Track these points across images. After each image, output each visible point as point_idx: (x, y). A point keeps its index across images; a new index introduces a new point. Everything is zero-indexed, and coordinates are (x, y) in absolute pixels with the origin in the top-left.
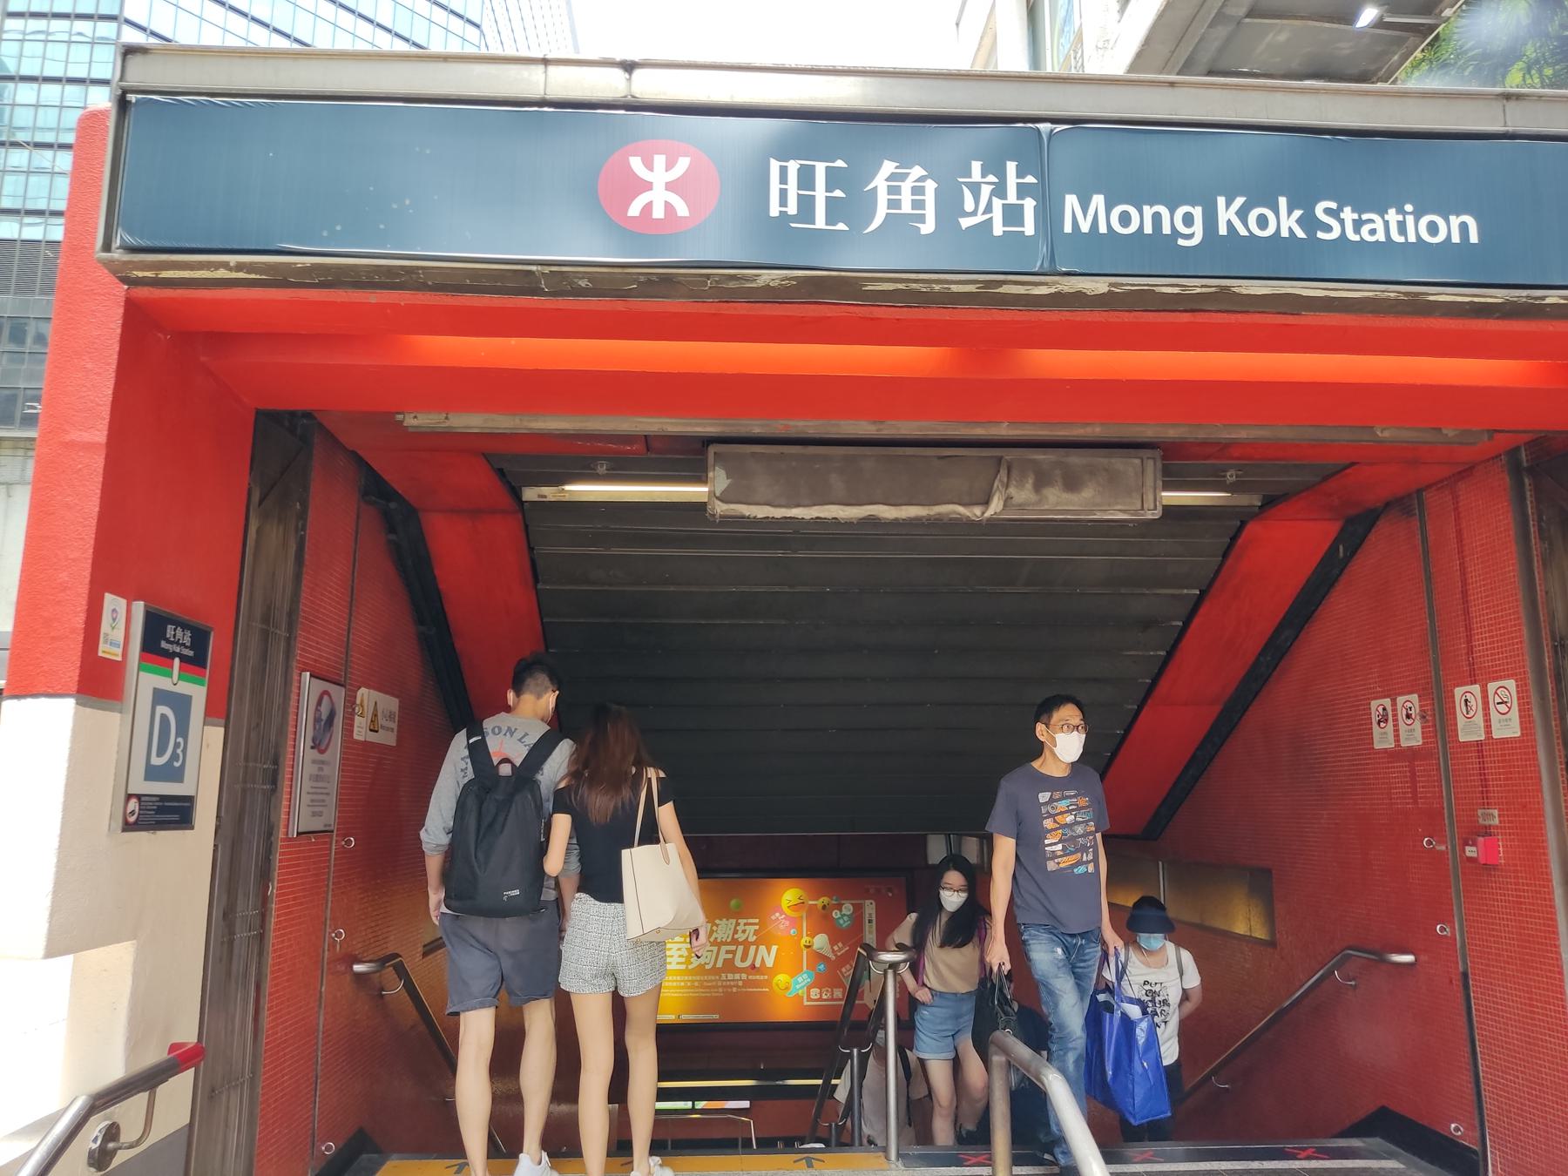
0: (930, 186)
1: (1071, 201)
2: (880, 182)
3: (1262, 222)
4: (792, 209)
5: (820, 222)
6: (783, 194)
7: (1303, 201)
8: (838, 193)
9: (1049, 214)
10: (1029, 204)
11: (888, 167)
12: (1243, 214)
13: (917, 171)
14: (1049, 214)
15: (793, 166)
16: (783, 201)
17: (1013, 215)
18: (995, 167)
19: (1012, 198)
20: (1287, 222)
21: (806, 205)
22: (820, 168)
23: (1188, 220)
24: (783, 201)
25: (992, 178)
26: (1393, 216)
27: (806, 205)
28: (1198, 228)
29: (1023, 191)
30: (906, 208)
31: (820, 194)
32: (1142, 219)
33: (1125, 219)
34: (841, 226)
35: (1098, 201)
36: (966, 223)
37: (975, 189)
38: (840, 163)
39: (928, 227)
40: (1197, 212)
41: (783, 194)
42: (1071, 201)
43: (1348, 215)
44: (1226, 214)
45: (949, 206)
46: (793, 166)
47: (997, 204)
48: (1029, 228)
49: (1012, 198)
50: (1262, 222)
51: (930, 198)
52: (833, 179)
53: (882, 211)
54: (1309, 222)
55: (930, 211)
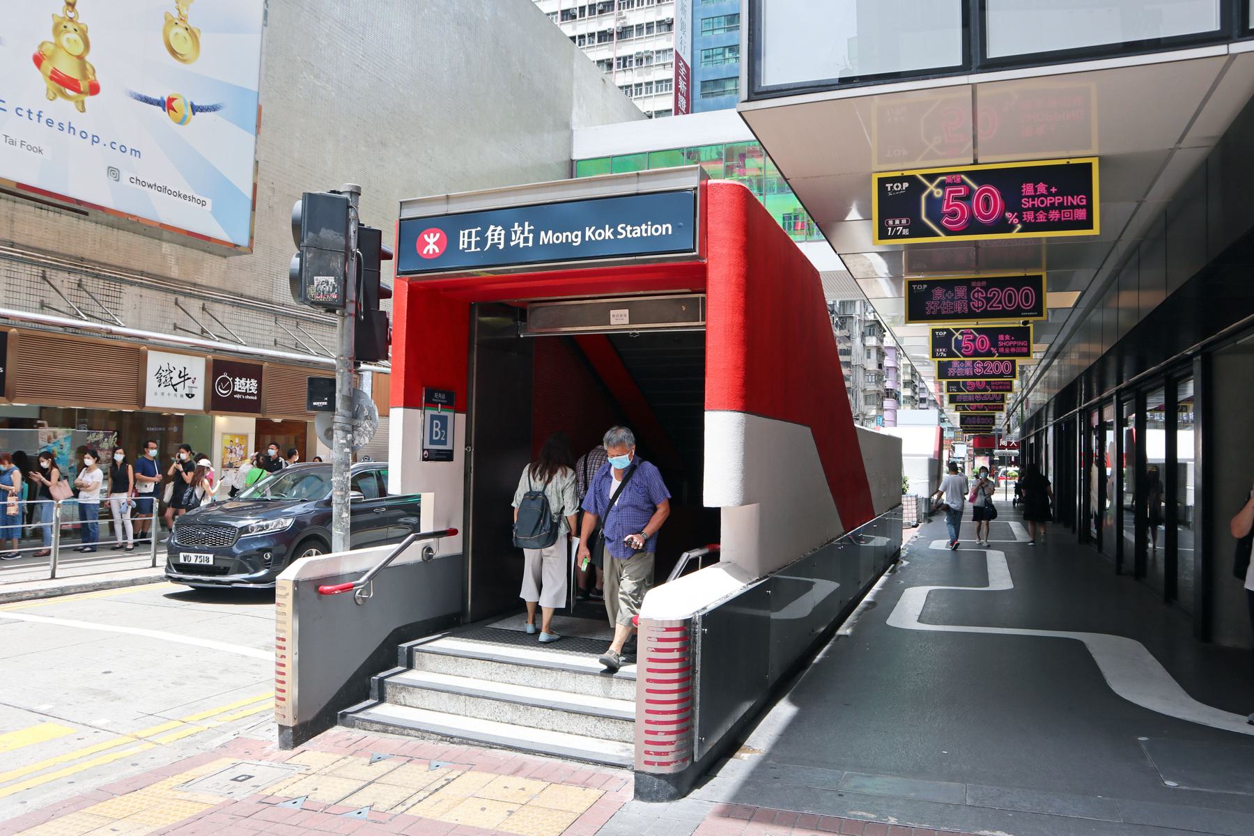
1: (543, 233)
2: (489, 233)
3: (600, 235)
7: (614, 226)
9: (537, 238)
10: (531, 236)
11: (492, 227)
12: (594, 233)
14: (537, 238)
20: (608, 234)
21: (469, 243)
22: (474, 231)
23: (576, 236)
26: (644, 227)
27: (469, 243)
28: (579, 239)
29: (529, 232)
31: (473, 240)
32: (562, 237)
33: (558, 238)
35: (550, 232)
36: (512, 244)
39: (501, 247)
40: (579, 233)
42: (543, 233)
43: (629, 228)
44: (588, 233)
45: (508, 239)
48: (530, 244)
50: (600, 235)
51: (502, 237)
52: (477, 234)
53: (490, 242)
54: (616, 233)
55: (502, 241)
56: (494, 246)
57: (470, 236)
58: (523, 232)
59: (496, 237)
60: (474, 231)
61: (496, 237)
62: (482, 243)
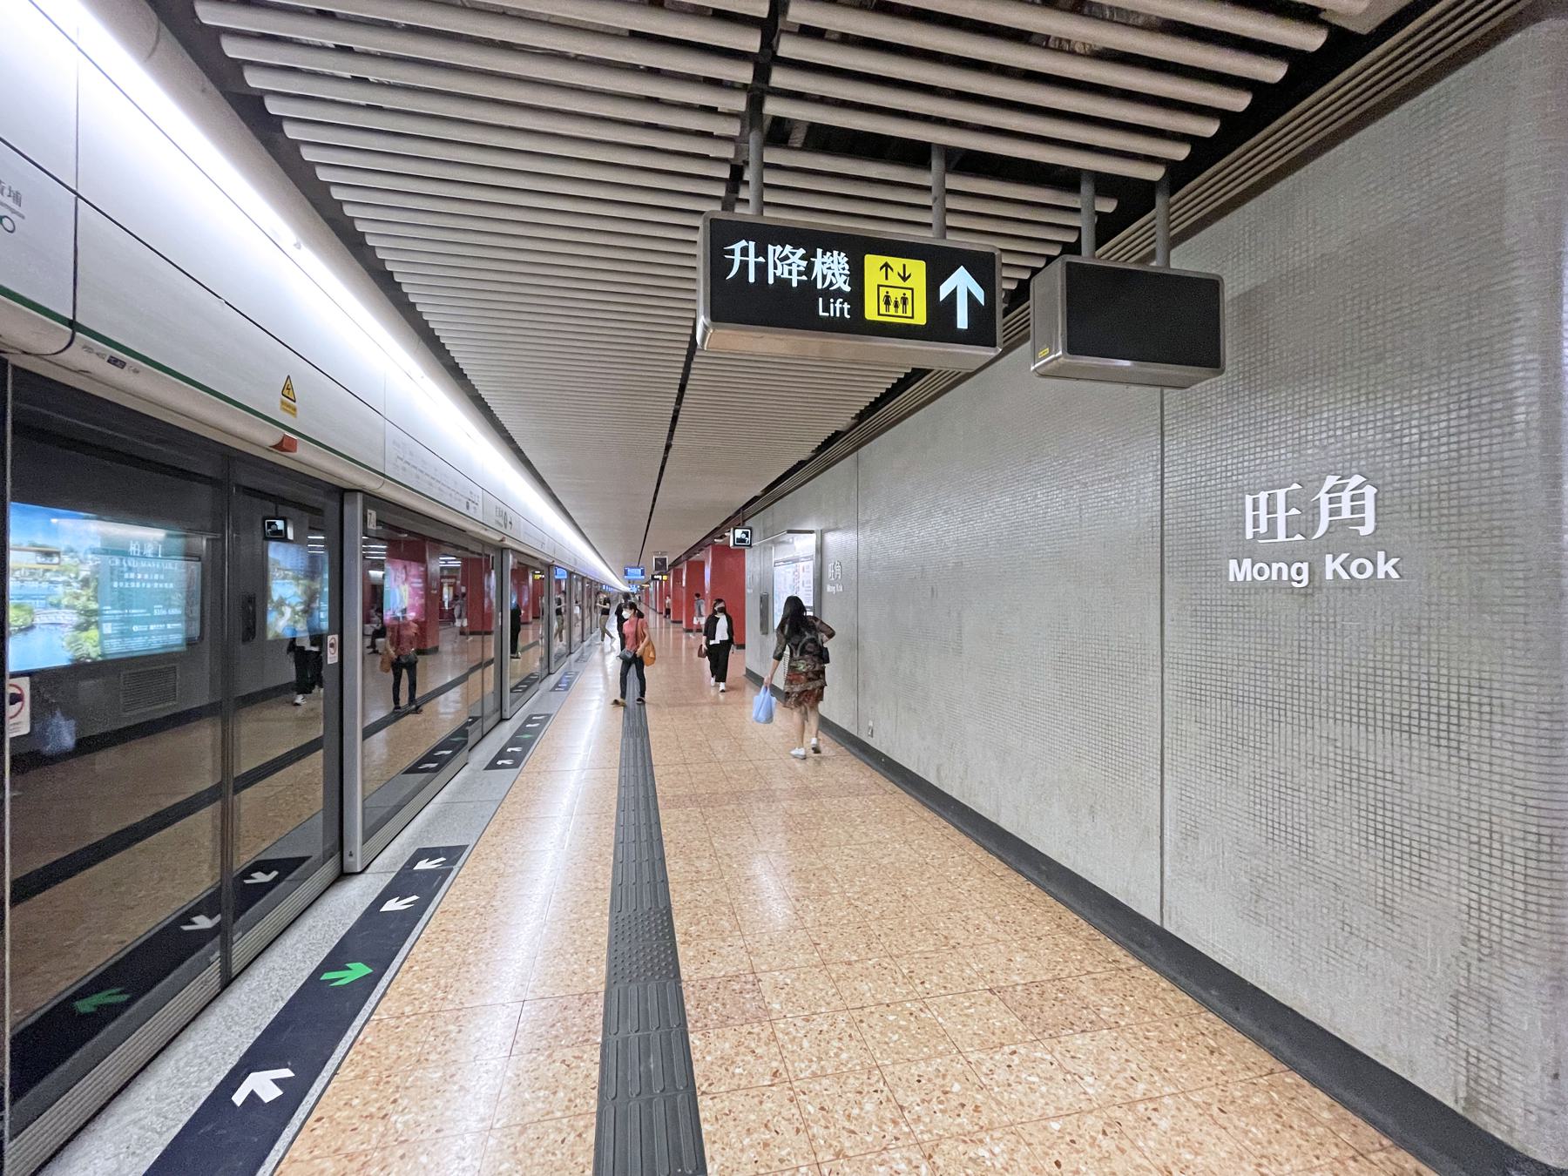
0: (1370, 491)
4: (1263, 529)
5: (1281, 537)
6: (1256, 519)
8: (1294, 511)
13: (1357, 480)
16: (1256, 525)
21: (1272, 523)
22: (1281, 494)
24: (1256, 525)
27: (1272, 523)
31: (1281, 516)
38: (1295, 486)
41: (1256, 519)
46: (1263, 496)
55: (1369, 514)
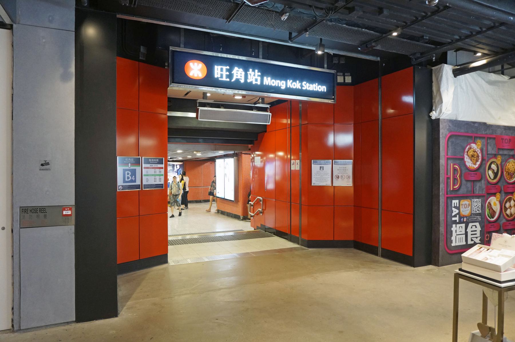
3: (294, 85)
4: (219, 76)
8: (228, 73)
12: (291, 83)
15: (219, 67)
17: (256, 80)
18: (254, 71)
19: (256, 77)
21: (222, 76)
23: (283, 84)
25: (253, 73)
30: (239, 77)
34: (228, 80)
36: (249, 81)
37: (250, 74)
43: (308, 84)
47: (254, 78)
49: (256, 77)
50: (294, 85)
52: (227, 70)
56: (238, 80)
57: (222, 70)
58: (254, 75)
59: (239, 75)
60: (225, 68)
61: (239, 75)
62: (230, 76)
